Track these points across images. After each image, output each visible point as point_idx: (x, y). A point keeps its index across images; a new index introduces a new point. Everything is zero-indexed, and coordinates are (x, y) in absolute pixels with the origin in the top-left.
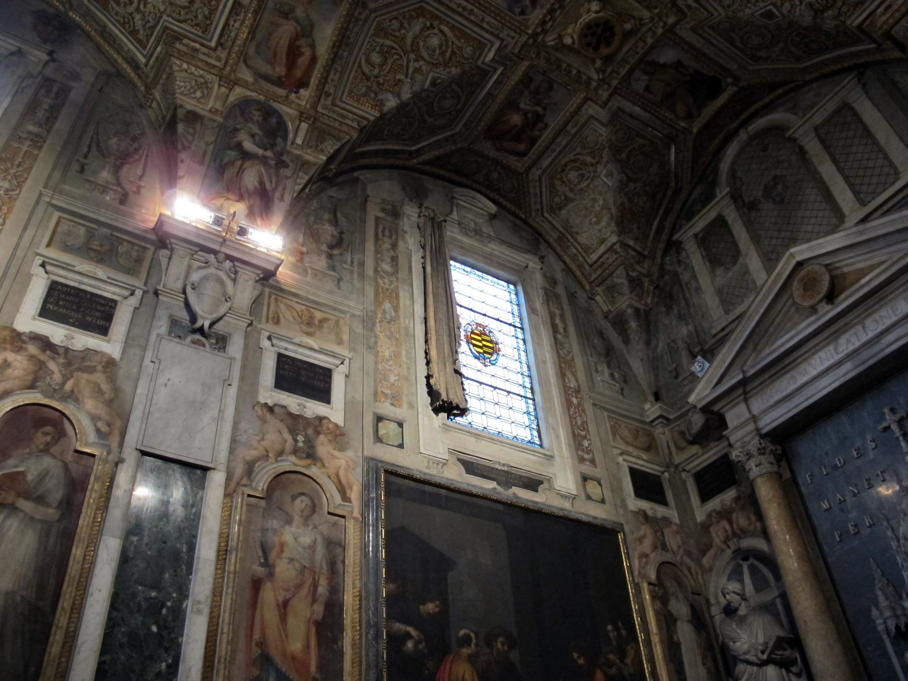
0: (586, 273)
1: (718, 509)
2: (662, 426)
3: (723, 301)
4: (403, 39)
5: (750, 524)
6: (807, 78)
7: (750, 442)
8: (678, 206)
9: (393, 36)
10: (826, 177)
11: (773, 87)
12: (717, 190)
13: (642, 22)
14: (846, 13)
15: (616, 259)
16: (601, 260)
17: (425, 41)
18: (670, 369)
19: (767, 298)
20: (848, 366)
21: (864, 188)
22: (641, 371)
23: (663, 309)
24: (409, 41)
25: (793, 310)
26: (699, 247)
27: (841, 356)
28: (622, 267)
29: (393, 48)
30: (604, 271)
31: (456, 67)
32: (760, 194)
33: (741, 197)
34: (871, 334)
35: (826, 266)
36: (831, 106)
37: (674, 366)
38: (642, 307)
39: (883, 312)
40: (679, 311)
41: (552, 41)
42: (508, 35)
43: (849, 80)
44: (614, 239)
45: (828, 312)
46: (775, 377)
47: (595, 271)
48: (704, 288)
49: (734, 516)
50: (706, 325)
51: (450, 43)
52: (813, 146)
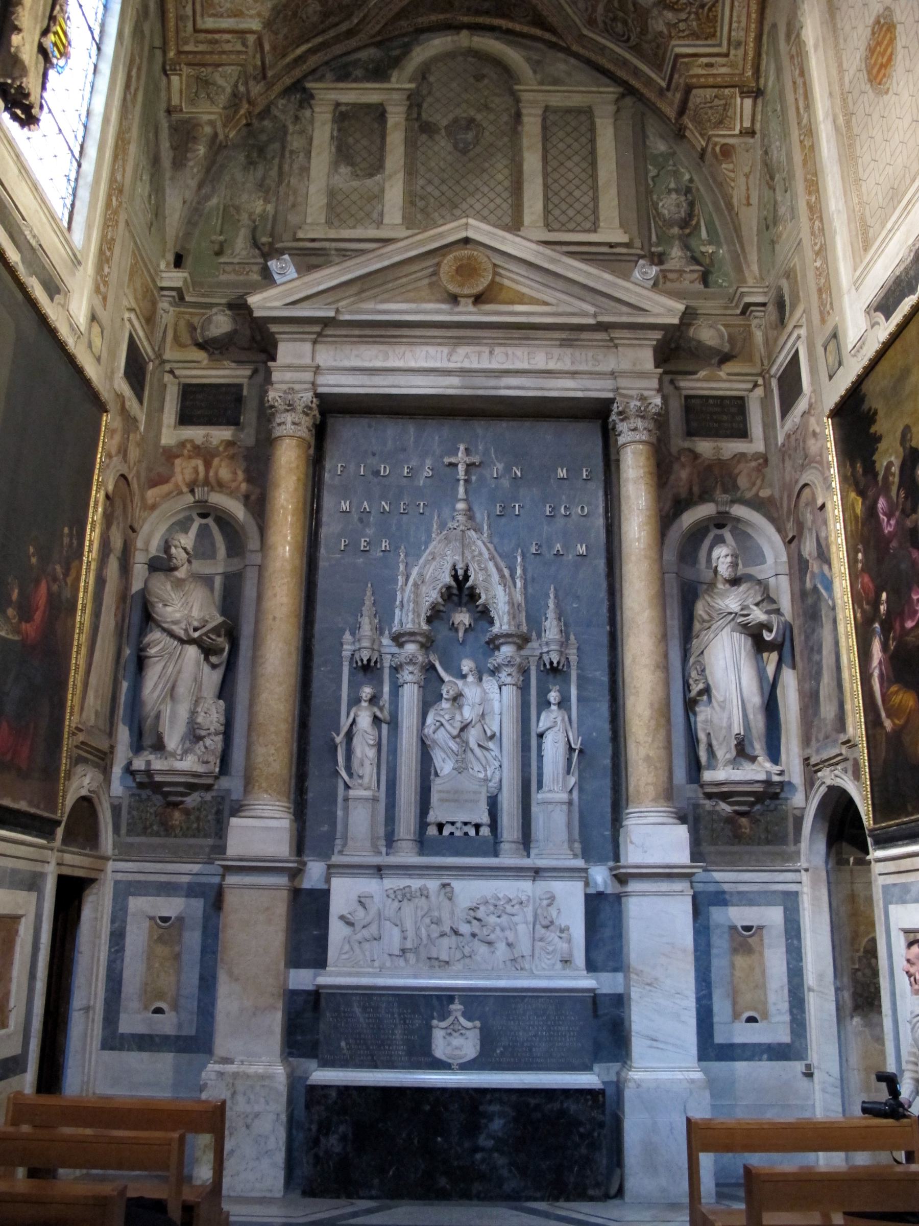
0: (182, 34)
1: (199, 442)
2: (171, 304)
3: (330, 207)
5: (234, 481)
6: (575, 48)
7: (298, 392)
8: (338, 49)
10: (526, 167)
11: (539, 21)
12: (395, 75)
14: (680, 31)
15: (239, 52)
16: (217, 36)
18: (214, 238)
19: (411, 250)
20: (455, 381)
21: (557, 212)
22: (177, 216)
23: (242, 158)
25: (426, 281)
26: (334, 121)
27: (452, 365)
28: (239, 68)
30: (212, 53)
32: (444, 122)
33: (419, 106)
34: (494, 365)
35: (495, 265)
36: (576, 100)
37: (222, 238)
38: (221, 137)
39: (519, 352)
40: (264, 178)
43: (612, 90)
44: (255, 25)
45: (467, 313)
46: (364, 340)
47: (197, 42)
48: (313, 173)
49: (216, 461)
50: (293, 219)
52: (531, 125)
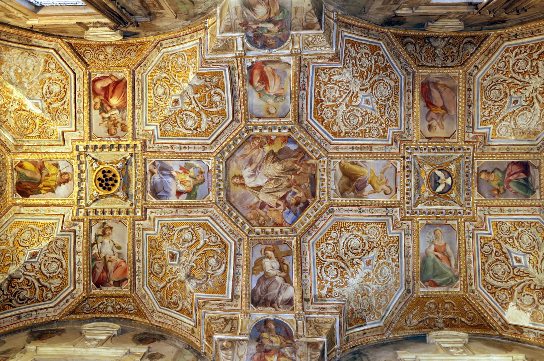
4: (208, 116)
9: (213, 115)
17: (195, 120)
24: (204, 116)
29: (210, 108)
31: (170, 116)
42: (153, 148)
51: (181, 126)
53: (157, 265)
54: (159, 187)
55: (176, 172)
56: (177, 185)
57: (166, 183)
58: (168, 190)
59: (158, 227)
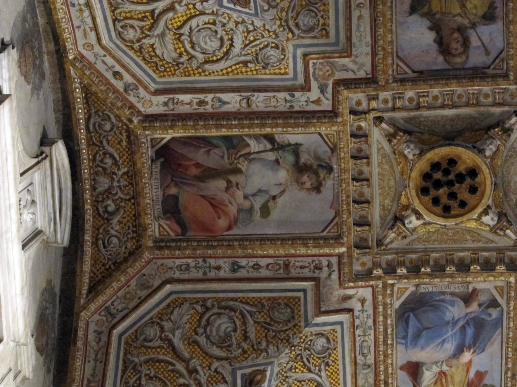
13: (392, 130)
41: (505, 235)
53: (229, 327)
54: (431, 316)
55: (470, 362)
56: (436, 363)
57: (440, 336)
58: (422, 341)
59: (324, 324)
